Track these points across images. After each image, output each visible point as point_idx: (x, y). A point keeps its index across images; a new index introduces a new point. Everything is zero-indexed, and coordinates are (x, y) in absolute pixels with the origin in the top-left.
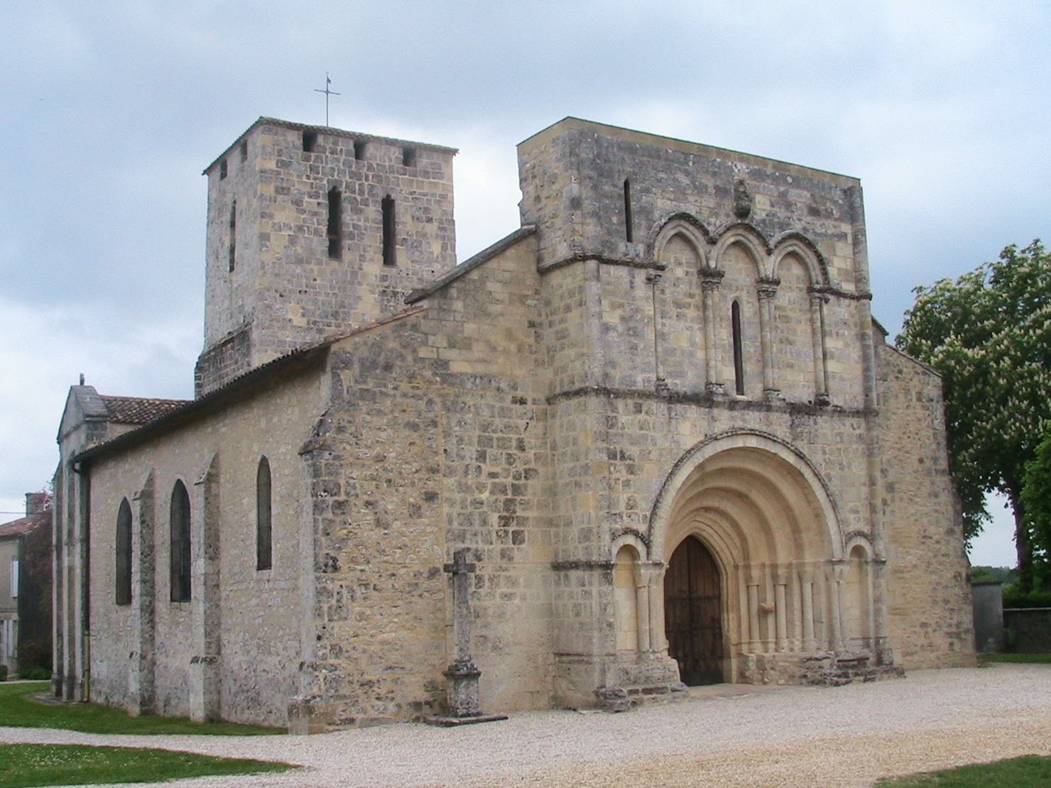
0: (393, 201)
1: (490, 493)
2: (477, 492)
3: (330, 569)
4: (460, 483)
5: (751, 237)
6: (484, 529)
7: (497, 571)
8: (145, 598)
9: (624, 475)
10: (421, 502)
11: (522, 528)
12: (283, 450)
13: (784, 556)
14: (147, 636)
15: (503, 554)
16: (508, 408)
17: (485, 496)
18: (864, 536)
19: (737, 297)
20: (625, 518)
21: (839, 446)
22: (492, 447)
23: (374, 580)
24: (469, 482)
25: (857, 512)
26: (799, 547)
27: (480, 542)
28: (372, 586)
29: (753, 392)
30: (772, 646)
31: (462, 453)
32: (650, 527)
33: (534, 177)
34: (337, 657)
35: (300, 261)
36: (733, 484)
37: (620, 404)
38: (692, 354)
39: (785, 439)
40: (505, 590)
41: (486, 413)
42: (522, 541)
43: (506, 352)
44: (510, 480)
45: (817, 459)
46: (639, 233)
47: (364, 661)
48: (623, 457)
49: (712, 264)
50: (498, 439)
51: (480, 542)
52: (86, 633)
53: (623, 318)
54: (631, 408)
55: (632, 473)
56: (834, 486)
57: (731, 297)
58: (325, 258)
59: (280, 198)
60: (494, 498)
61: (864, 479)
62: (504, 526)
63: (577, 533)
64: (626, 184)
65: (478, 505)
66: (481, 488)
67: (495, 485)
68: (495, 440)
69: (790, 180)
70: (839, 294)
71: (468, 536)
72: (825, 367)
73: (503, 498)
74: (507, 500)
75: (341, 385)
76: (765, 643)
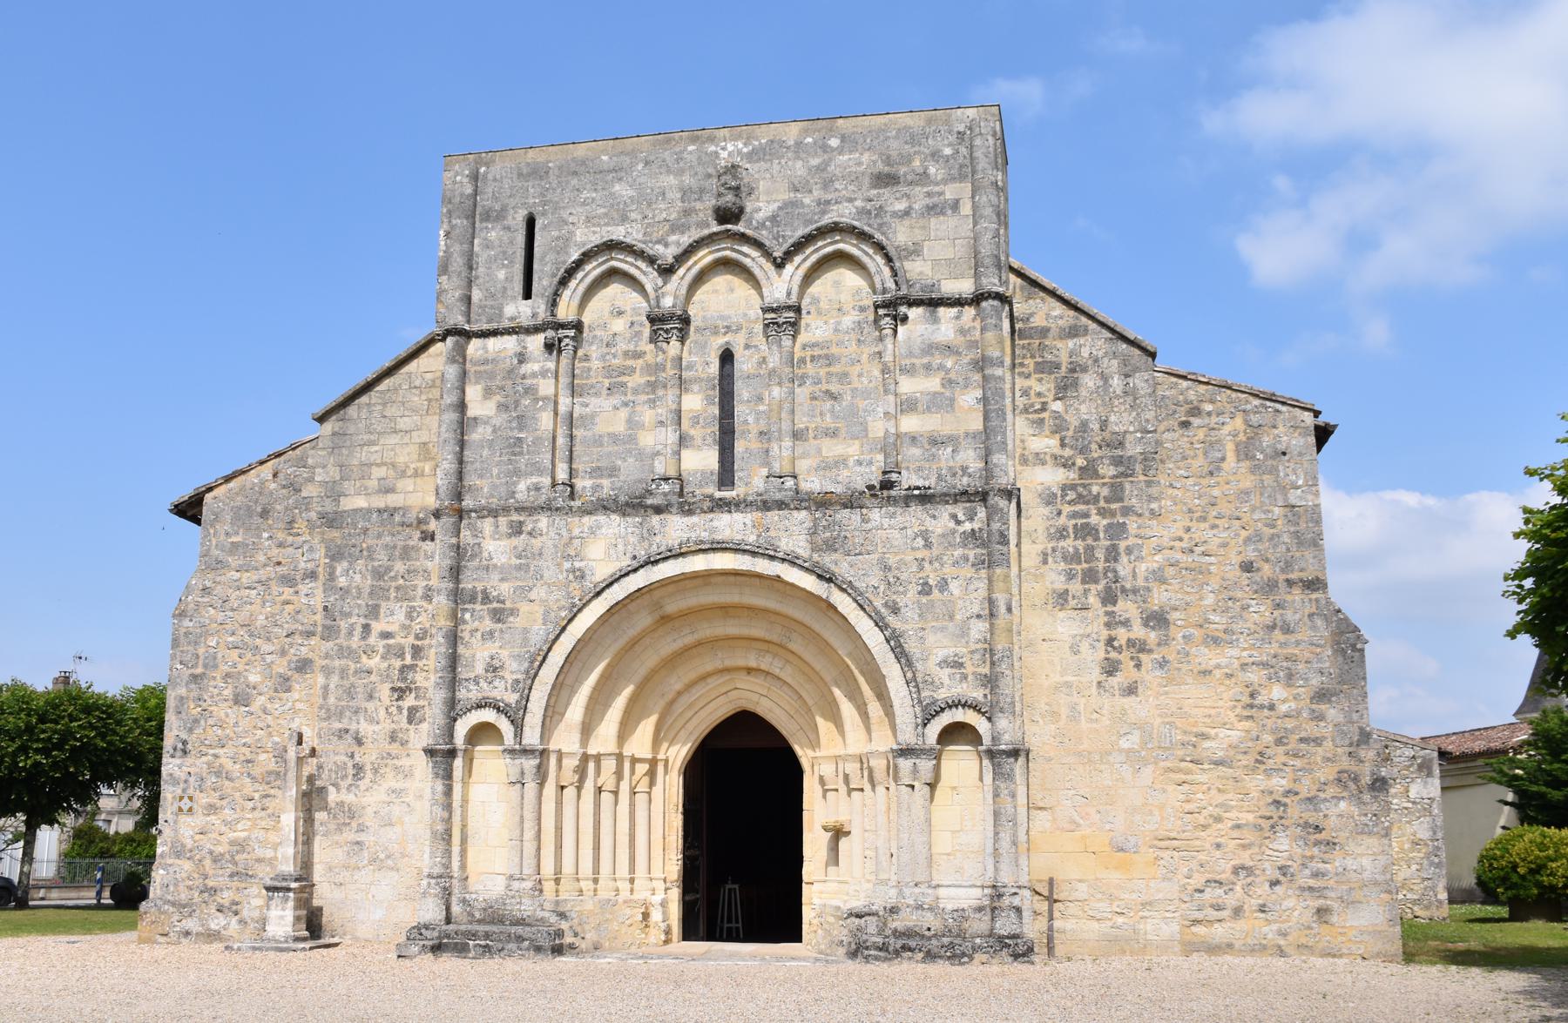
1: (382, 657)
2: (364, 658)
3: (179, 753)
4: (341, 648)
5: (745, 249)
6: (370, 706)
7: (382, 758)
9: (488, 624)
10: (290, 673)
11: (421, 703)
15: (393, 738)
16: (413, 547)
17: (374, 662)
18: (975, 708)
19: (727, 343)
20: (483, 684)
21: (919, 555)
23: (228, 764)
24: (354, 646)
27: (362, 720)
28: (224, 775)
29: (752, 480)
34: (178, 857)
37: (487, 525)
39: (801, 552)
40: (394, 784)
41: (382, 557)
44: (411, 640)
46: (542, 283)
47: (208, 862)
48: (486, 599)
50: (398, 588)
51: (362, 720)
53: (503, 407)
55: (499, 621)
56: (906, 623)
57: (718, 342)
60: (386, 665)
62: (397, 700)
65: (363, 675)
66: (369, 651)
67: (388, 647)
68: (392, 590)
69: (834, 143)
71: (348, 713)
73: (398, 663)
75: (210, 541)
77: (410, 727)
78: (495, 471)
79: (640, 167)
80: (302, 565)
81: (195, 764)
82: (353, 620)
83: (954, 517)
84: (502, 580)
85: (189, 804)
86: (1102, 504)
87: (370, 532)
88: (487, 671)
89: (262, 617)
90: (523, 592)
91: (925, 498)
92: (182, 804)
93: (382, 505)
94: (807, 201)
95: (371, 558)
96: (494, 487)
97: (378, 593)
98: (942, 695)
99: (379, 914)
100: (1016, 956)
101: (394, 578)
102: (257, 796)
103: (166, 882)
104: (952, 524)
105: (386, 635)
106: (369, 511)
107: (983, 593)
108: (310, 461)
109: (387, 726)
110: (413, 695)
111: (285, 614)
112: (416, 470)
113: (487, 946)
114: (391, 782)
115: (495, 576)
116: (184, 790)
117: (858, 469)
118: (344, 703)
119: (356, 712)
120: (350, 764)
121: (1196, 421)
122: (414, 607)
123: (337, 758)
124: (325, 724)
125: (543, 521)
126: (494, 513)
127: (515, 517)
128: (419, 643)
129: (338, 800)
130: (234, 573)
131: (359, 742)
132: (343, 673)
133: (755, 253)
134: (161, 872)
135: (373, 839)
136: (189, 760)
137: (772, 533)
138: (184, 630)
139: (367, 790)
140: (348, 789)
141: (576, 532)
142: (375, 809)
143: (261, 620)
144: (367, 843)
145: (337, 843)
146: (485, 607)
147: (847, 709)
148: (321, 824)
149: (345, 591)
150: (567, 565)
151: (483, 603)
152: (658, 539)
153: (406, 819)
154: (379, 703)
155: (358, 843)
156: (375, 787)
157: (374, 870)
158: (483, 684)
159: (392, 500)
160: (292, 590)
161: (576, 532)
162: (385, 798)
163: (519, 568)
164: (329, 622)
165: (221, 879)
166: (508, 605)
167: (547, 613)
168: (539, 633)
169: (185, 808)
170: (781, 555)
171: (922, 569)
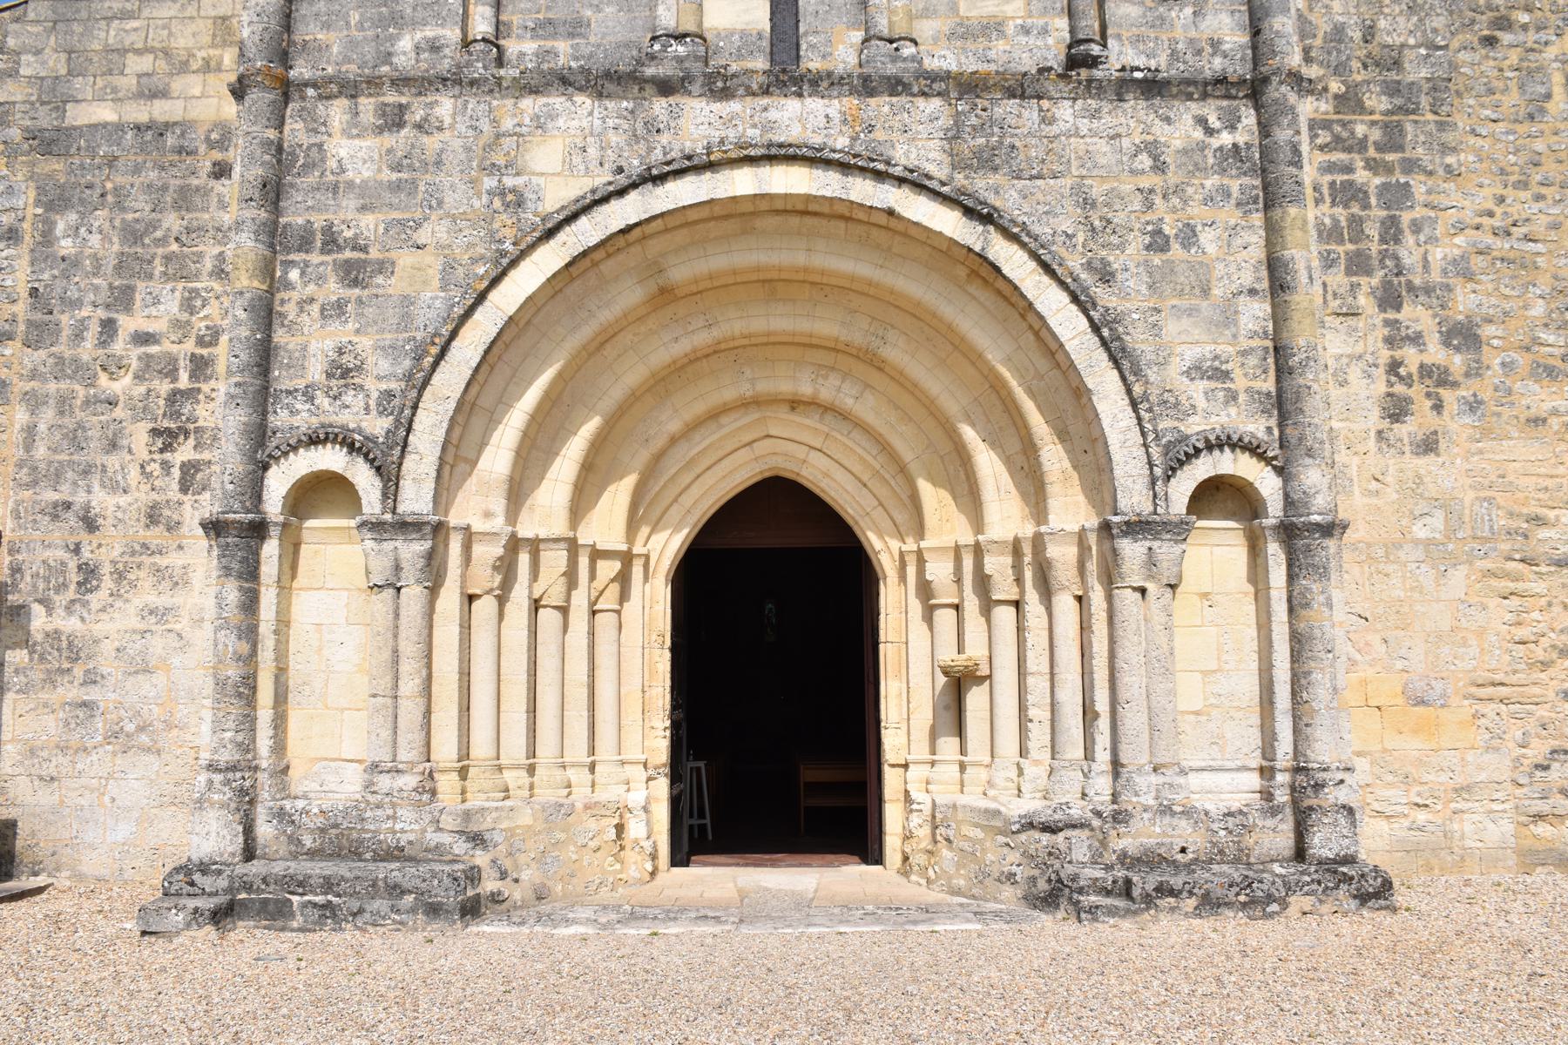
1: (136, 377)
2: (103, 379)
6: (113, 461)
7: (133, 553)
9: (333, 289)
11: (206, 456)
15: (153, 516)
16: (198, 189)
17: (120, 385)
18: (1254, 450)
21: (1145, 183)
22: (150, 276)
24: (85, 357)
27: (96, 487)
31: (73, 293)
36: (826, 325)
37: (337, 112)
39: (931, 168)
41: (140, 205)
44: (190, 346)
48: (331, 242)
50: (168, 259)
51: (96, 487)
55: (355, 283)
60: (142, 389)
62: (162, 451)
65: (100, 408)
66: (112, 367)
68: (157, 261)
71: (70, 475)
73: (164, 387)
77: (185, 498)
78: (355, 17)
82: (85, 312)
83: (1202, 121)
84: (363, 209)
86: (1372, 152)
87: (120, 164)
88: (329, 375)
90: (404, 231)
91: (1153, 87)
93: (143, 118)
95: (120, 206)
96: (352, 44)
97: (132, 267)
98: (1194, 426)
99: (123, 831)
100: (1363, 898)
101: (162, 242)
104: (1199, 134)
105: (143, 338)
106: (119, 127)
107: (1257, 252)
109: (142, 496)
110: (191, 442)
112: (207, 61)
113: (327, 905)
114: (147, 594)
115: (350, 203)
117: (1023, 39)
118: (64, 457)
119: (86, 473)
120: (72, 565)
121: (1506, 38)
122: (196, 291)
123: (48, 553)
124: (27, 494)
125: (445, 106)
126: (350, 89)
127: (391, 98)
128: (205, 352)
129: (49, 628)
131: (90, 524)
132: (64, 404)
135: (112, 696)
137: (879, 135)
139: (103, 610)
140: (67, 608)
141: (508, 124)
142: (117, 644)
144: (101, 704)
145: (45, 705)
146: (328, 258)
147: (989, 465)
148: (17, 671)
149: (71, 264)
150: (489, 182)
151: (323, 252)
152: (664, 139)
153: (176, 661)
154: (129, 457)
155: (84, 704)
156: (118, 604)
157: (114, 754)
158: (322, 401)
159: (161, 110)
161: (508, 124)
162: (135, 623)
163: (396, 187)
164: (38, 316)
166: (374, 254)
167: (449, 268)
168: (432, 305)
170: (898, 171)
171: (1150, 206)
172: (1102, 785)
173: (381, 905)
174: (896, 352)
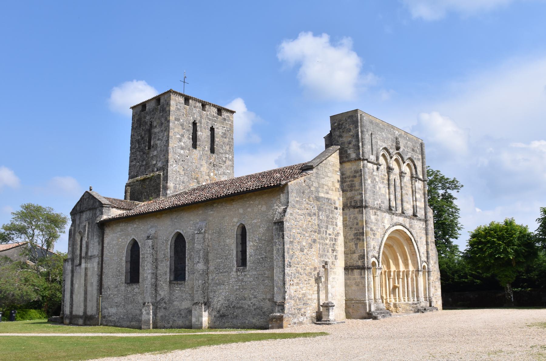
0: (214, 129)
3: (289, 266)
6: (328, 254)
8: (153, 280)
9: (372, 237)
11: (337, 254)
12: (255, 221)
13: (402, 268)
14: (154, 295)
17: (327, 242)
25: (424, 254)
26: (406, 265)
30: (397, 300)
32: (379, 255)
33: (339, 129)
35: (182, 148)
38: (385, 196)
41: (328, 212)
42: (337, 259)
43: (332, 190)
45: (415, 235)
46: (375, 152)
47: (298, 300)
49: (391, 165)
50: (331, 221)
52: (101, 296)
54: (373, 213)
57: (394, 176)
58: (191, 148)
59: (176, 122)
60: (330, 243)
61: (425, 243)
63: (358, 257)
64: (371, 134)
67: (330, 238)
69: (408, 138)
70: (420, 179)
72: (416, 203)
73: (332, 243)
74: (333, 244)
76: (395, 299)
79: (386, 130)
80: (313, 211)
81: (293, 269)
82: (323, 229)
84: (374, 226)
85: (293, 282)
87: (325, 204)
89: (305, 225)
91: (420, 220)
92: (291, 282)
94: (406, 150)
102: (307, 279)
103: (289, 307)
105: (330, 235)
106: (325, 198)
108: (312, 180)
111: (309, 225)
113: (384, 315)
116: (291, 278)
118: (323, 253)
124: (320, 259)
130: (297, 210)
133: (401, 159)
134: (288, 304)
136: (291, 269)
137: (405, 223)
138: (287, 226)
143: (304, 226)
160: (310, 218)
164: (319, 229)
165: (301, 305)
166: (375, 232)
168: (380, 240)
169: (292, 284)
172: (416, 299)
173: (387, 315)
174: (395, 247)
